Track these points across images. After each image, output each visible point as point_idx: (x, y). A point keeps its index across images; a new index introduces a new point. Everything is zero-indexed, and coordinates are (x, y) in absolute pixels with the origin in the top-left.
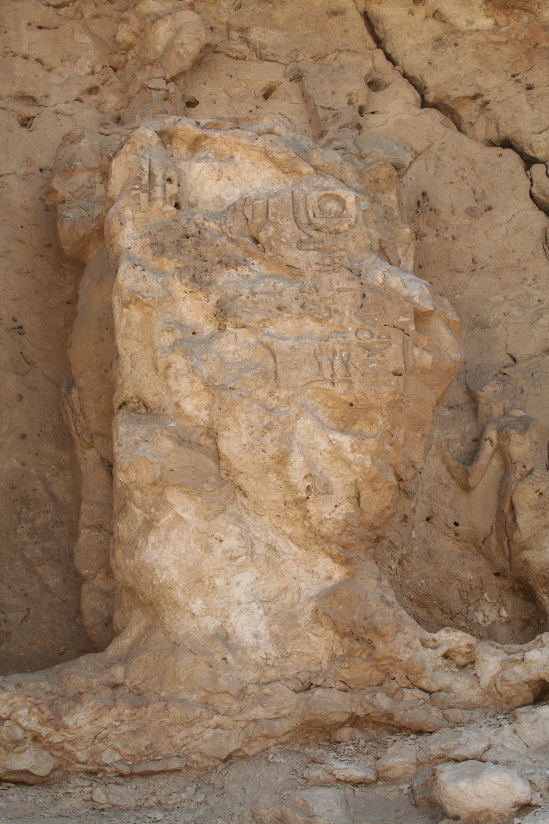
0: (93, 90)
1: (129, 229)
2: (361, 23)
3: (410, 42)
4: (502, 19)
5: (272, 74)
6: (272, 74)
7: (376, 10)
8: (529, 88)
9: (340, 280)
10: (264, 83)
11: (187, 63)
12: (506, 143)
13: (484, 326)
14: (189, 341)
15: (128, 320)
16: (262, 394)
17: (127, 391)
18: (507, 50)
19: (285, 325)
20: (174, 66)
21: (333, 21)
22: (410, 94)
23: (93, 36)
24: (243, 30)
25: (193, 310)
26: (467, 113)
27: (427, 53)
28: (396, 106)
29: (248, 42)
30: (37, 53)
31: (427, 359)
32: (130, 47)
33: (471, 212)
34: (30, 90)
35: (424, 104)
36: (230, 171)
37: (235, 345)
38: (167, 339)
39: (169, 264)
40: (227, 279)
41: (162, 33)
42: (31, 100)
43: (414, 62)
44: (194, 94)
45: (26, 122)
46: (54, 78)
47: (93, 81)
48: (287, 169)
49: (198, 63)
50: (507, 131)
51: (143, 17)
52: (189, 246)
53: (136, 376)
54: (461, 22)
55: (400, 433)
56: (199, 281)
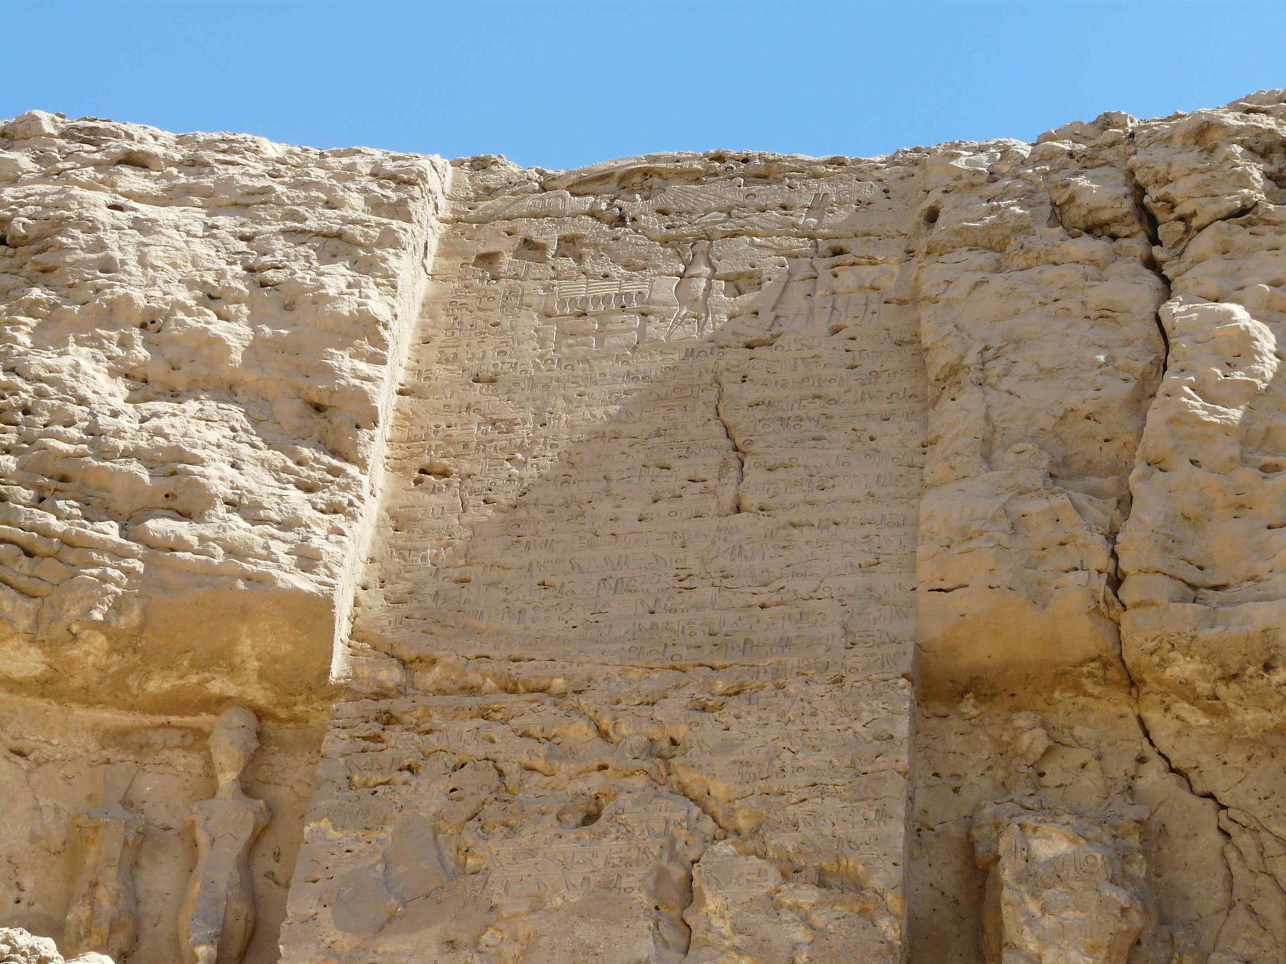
0: (990, 768)
1: (1007, 872)
2: (1136, 722)
3: (1163, 733)
4: (1214, 720)
5: (1086, 755)
6: (1086, 755)
7: (1145, 715)
8: (1225, 763)
9: (1091, 894)
10: (1080, 761)
11: (1039, 756)
12: (1210, 796)
13: (1187, 899)
14: (1031, 920)
15: (1007, 911)
16: (1058, 941)
17: (1008, 940)
18: (1215, 739)
19: (1069, 914)
20: (1032, 759)
21: (1121, 721)
22: (1161, 764)
23: (989, 736)
24: (1071, 728)
25: (1033, 907)
26: (1193, 775)
27: (1172, 740)
28: (1153, 775)
29: (1073, 736)
30: (959, 749)
31: (1125, 927)
32: (1009, 744)
33: (1186, 836)
34: (957, 771)
35: (1172, 770)
36: (1050, 842)
37: (1049, 922)
38: (1022, 919)
39: (1023, 888)
40: (1046, 893)
41: (1026, 739)
42: (956, 776)
43: (1164, 746)
44: (1043, 769)
45: (956, 790)
46: (970, 763)
47: (990, 763)
48: (1073, 841)
49: (1044, 755)
50: (1210, 789)
51: (1016, 729)
52: (1034, 879)
53: (1011, 933)
54: (1192, 720)
55: (1113, 957)
56: (1035, 896)
